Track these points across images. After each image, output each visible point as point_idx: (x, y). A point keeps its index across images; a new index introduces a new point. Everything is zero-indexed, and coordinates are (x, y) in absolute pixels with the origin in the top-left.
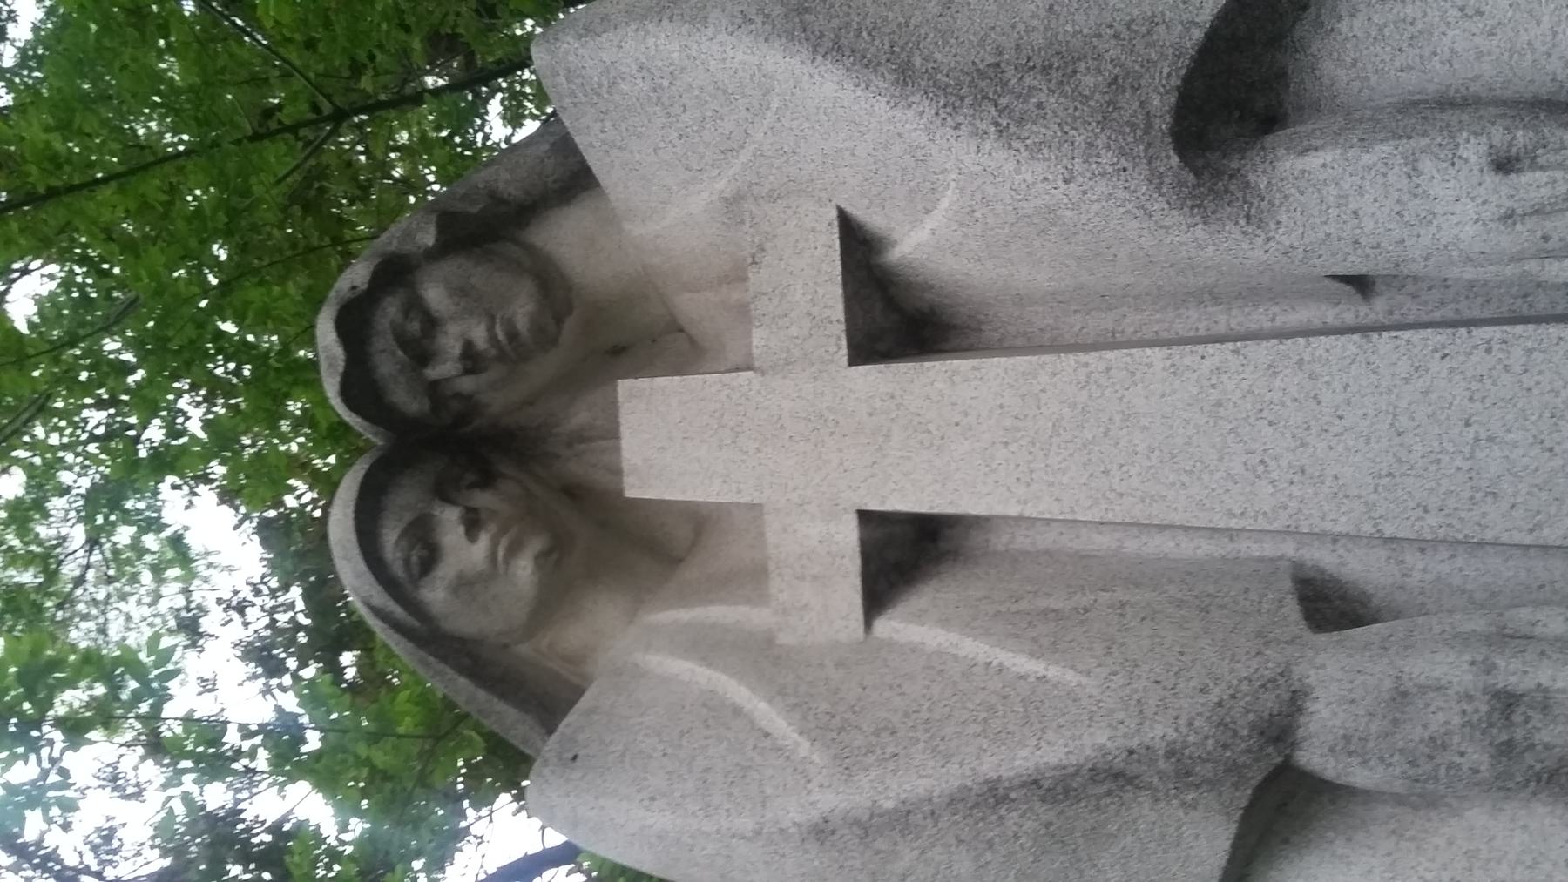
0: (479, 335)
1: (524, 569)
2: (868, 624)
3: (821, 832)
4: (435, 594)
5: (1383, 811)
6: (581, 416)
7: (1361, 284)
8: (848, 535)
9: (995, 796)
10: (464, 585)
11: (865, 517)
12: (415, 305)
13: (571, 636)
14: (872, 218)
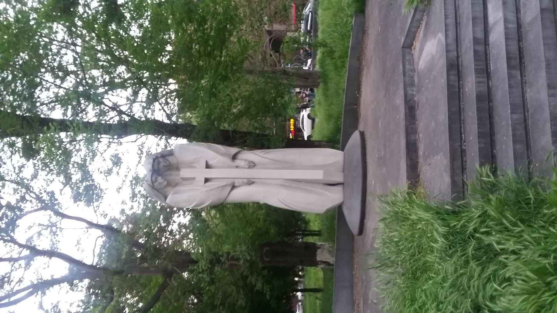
0: (165, 165)
1: (165, 183)
2: (205, 183)
3: (206, 191)
4: (156, 184)
5: (237, 188)
6: (167, 173)
7: (237, 167)
8: (204, 179)
9: (219, 187)
10: (160, 184)
11: (205, 178)
12: (159, 160)
13: (167, 190)
14: (208, 160)
